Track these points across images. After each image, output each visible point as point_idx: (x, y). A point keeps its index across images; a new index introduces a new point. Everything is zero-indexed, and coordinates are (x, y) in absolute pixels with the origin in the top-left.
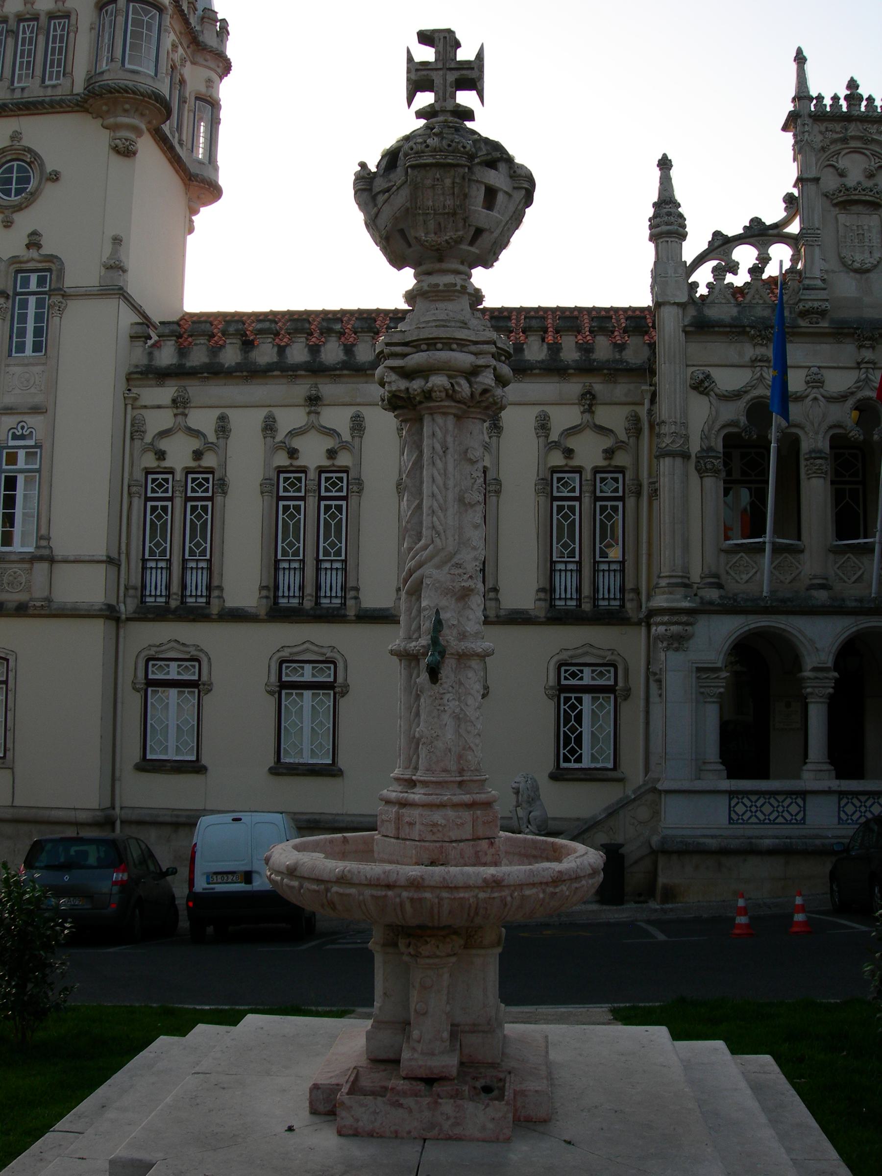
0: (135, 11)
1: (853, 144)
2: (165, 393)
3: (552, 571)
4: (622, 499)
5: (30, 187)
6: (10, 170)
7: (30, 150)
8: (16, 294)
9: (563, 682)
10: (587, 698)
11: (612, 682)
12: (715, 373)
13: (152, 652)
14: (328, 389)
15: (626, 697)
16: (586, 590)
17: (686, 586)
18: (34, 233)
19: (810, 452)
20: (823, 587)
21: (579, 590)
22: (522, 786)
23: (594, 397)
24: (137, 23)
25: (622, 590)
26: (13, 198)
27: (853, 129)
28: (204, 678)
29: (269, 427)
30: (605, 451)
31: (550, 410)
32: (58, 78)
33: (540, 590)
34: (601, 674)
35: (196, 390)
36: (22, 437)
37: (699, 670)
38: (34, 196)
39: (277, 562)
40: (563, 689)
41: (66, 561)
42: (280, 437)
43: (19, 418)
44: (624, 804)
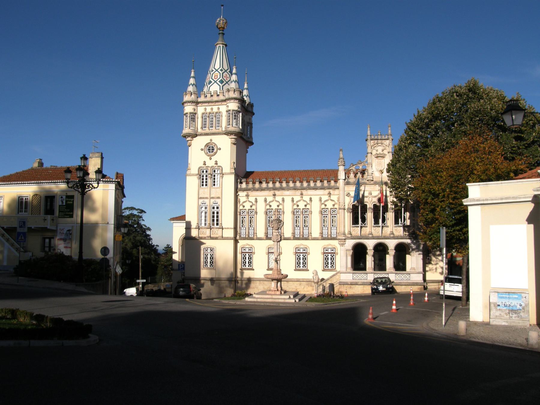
0: (235, 113)
1: (379, 144)
2: (245, 193)
3: (323, 229)
4: (336, 214)
5: (215, 151)
6: (210, 147)
7: (214, 143)
8: (213, 174)
9: (325, 252)
10: (330, 255)
11: (334, 252)
12: (350, 192)
13: (243, 247)
14: (277, 192)
15: (337, 254)
16: (329, 233)
17: (344, 234)
18: (216, 161)
19: (369, 208)
20: (370, 234)
21: (328, 233)
22: (314, 272)
23: (331, 194)
24: (235, 116)
25: (336, 233)
26: (211, 153)
27: (379, 141)
28: (253, 251)
29: (266, 200)
30: (333, 205)
31: (322, 196)
32: (219, 127)
33: (320, 233)
34: (332, 250)
35: (250, 193)
36: (215, 204)
37: (346, 250)
38: (216, 153)
39: (267, 228)
40: (324, 253)
41: (225, 228)
42: (267, 203)
43: (215, 199)
44: (334, 275)
